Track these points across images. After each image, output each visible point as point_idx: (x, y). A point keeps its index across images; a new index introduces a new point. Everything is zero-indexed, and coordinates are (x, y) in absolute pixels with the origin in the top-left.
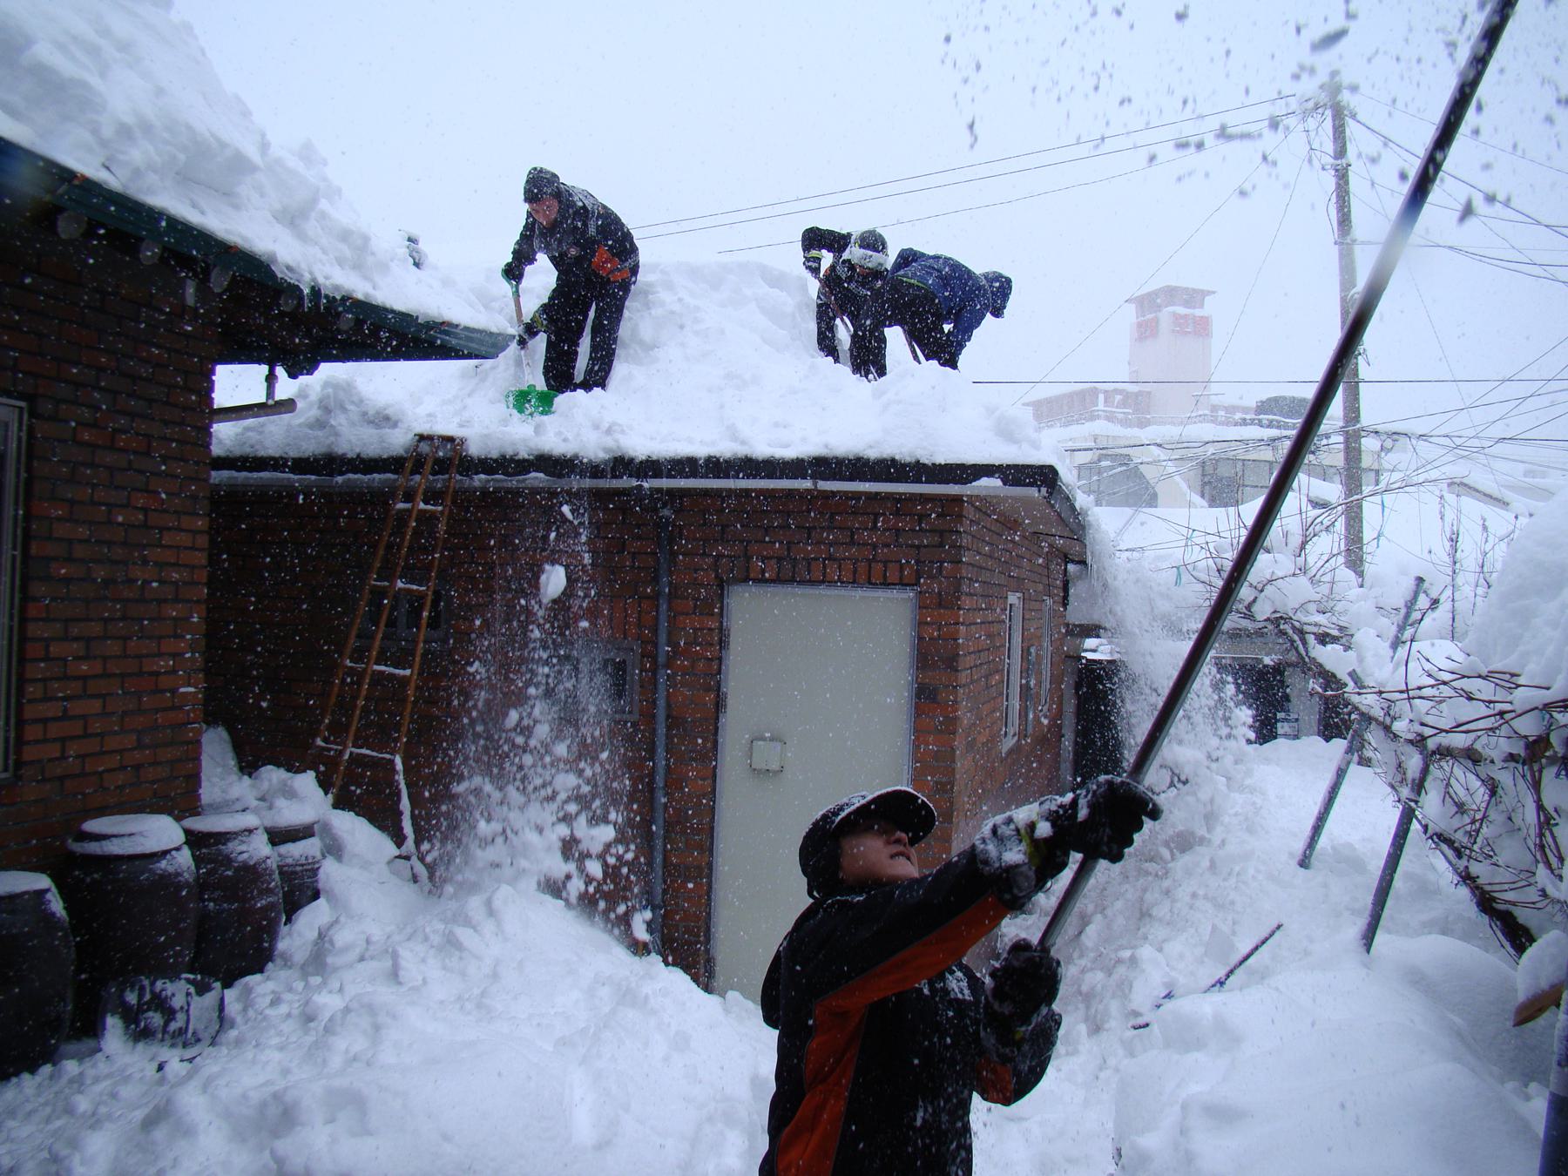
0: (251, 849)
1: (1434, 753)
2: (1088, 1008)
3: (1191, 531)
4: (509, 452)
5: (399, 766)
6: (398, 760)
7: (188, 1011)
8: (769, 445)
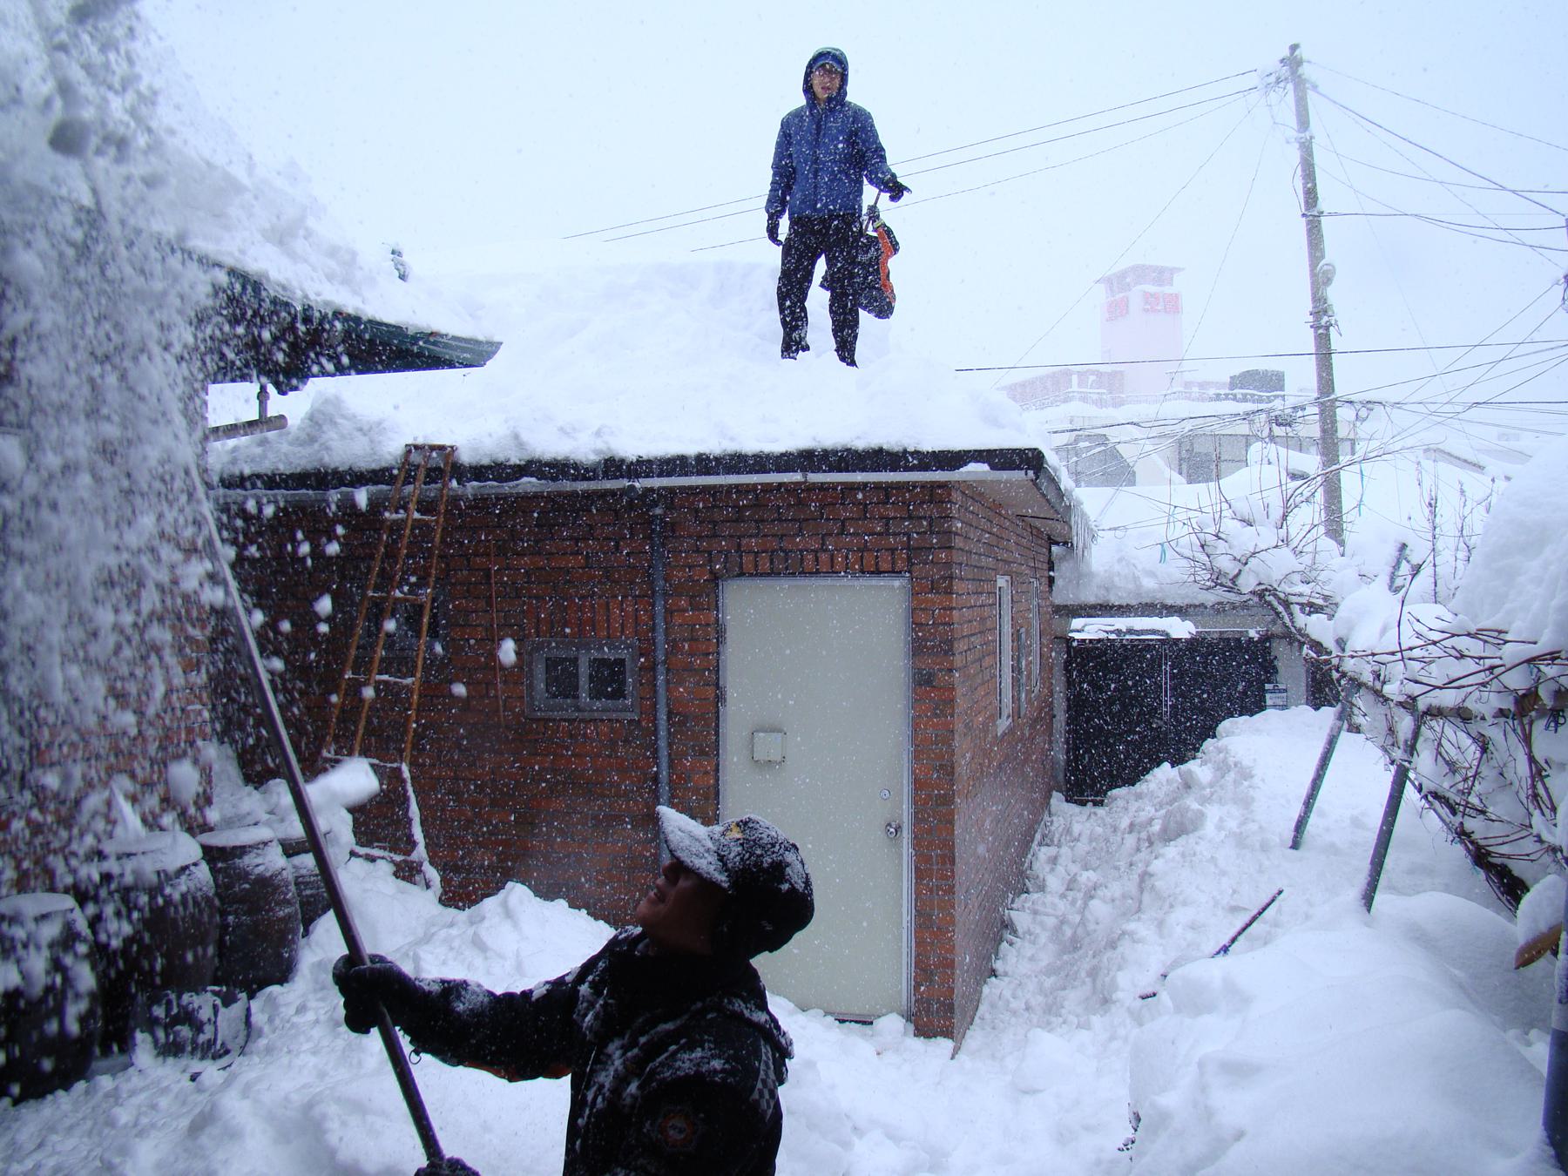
0: (266, 861)
1: (1425, 713)
2: (1094, 981)
3: (1173, 508)
4: (501, 458)
5: (406, 774)
6: (405, 768)
7: (215, 1022)
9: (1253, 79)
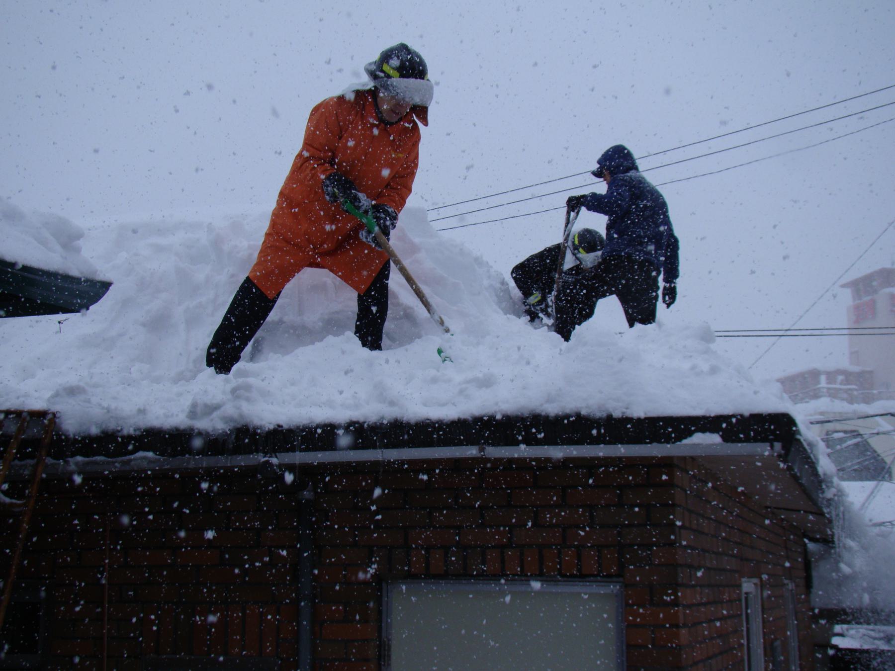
4: (112, 426)
8: (425, 405)
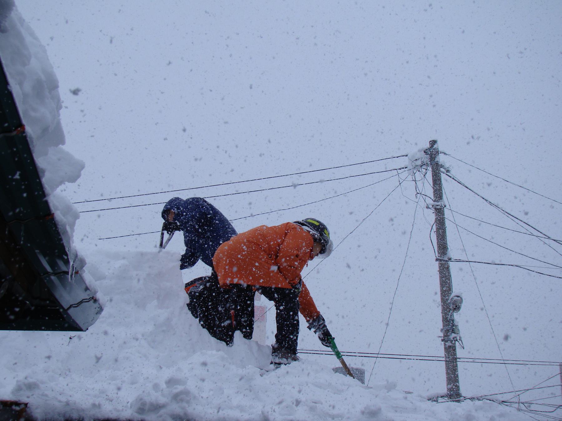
9: (404, 162)
